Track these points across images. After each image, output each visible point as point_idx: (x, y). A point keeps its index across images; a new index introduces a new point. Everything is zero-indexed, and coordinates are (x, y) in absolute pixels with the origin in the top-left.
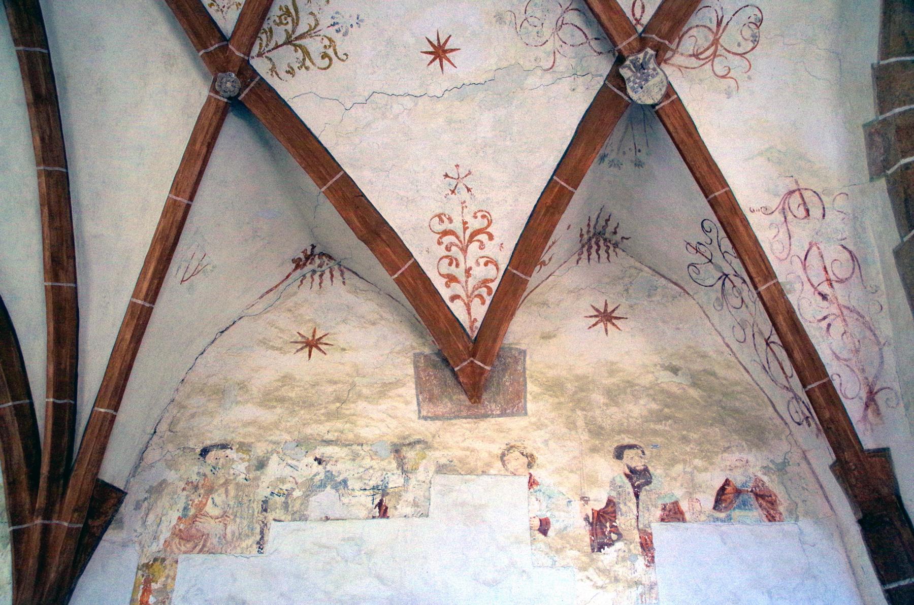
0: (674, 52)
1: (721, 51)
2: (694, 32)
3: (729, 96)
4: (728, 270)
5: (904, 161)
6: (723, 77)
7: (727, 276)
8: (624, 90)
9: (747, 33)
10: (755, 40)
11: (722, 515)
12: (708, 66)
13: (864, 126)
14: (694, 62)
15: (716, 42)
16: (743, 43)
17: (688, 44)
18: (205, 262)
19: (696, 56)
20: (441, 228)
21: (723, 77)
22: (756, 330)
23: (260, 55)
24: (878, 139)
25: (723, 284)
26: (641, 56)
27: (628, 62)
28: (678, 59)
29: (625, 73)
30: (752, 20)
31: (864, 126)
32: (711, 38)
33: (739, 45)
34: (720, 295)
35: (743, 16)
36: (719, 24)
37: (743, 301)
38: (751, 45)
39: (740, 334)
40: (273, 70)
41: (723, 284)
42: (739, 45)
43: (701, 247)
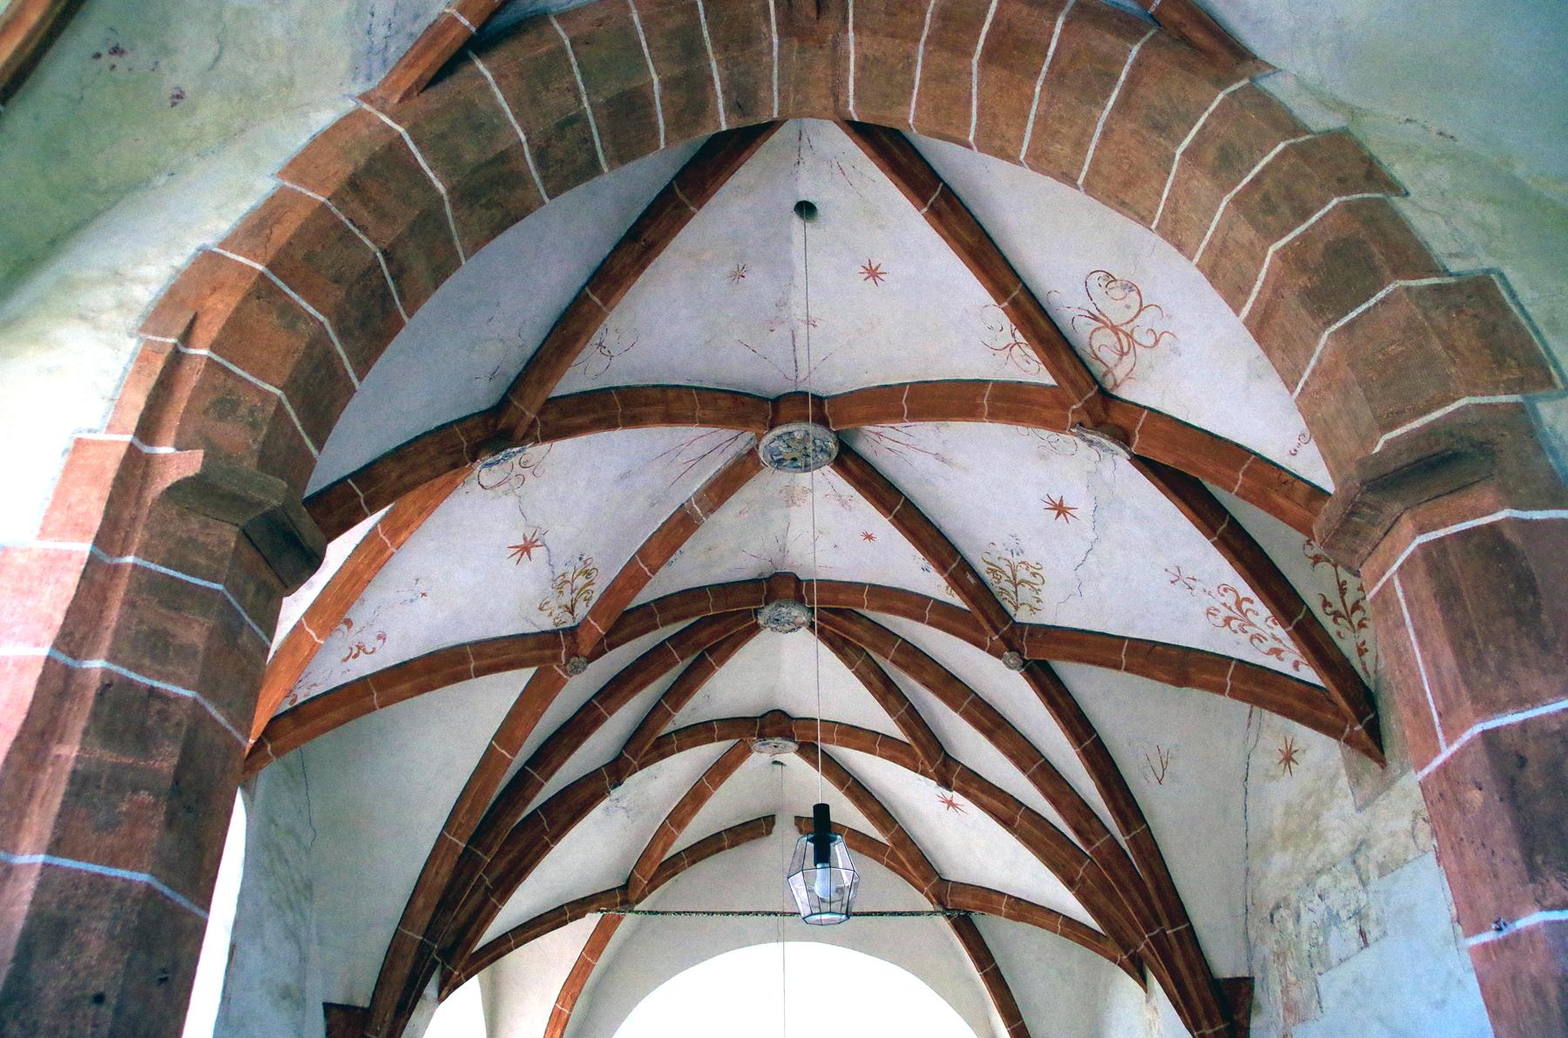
0: (1109, 371)
1: (1127, 329)
2: (1096, 345)
3: (1177, 352)
6: (1157, 342)
9: (1118, 293)
10: (1130, 287)
12: (1138, 349)
14: (1128, 361)
15: (1115, 329)
16: (1127, 301)
17: (1109, 357)
18: (1164, 750)
19: (1122, 354)
20: (1220, 621)
21: (1157, 342)
23: (1016, 608)
28: (1120, 373)
30: (1104, 284)
32: (1108, 331)
33: (1128, 307)
35: (1096, 291)
36: (1095, 318)
38: (1134, 294)
40: (1032, 609)
42: (1128, 307)
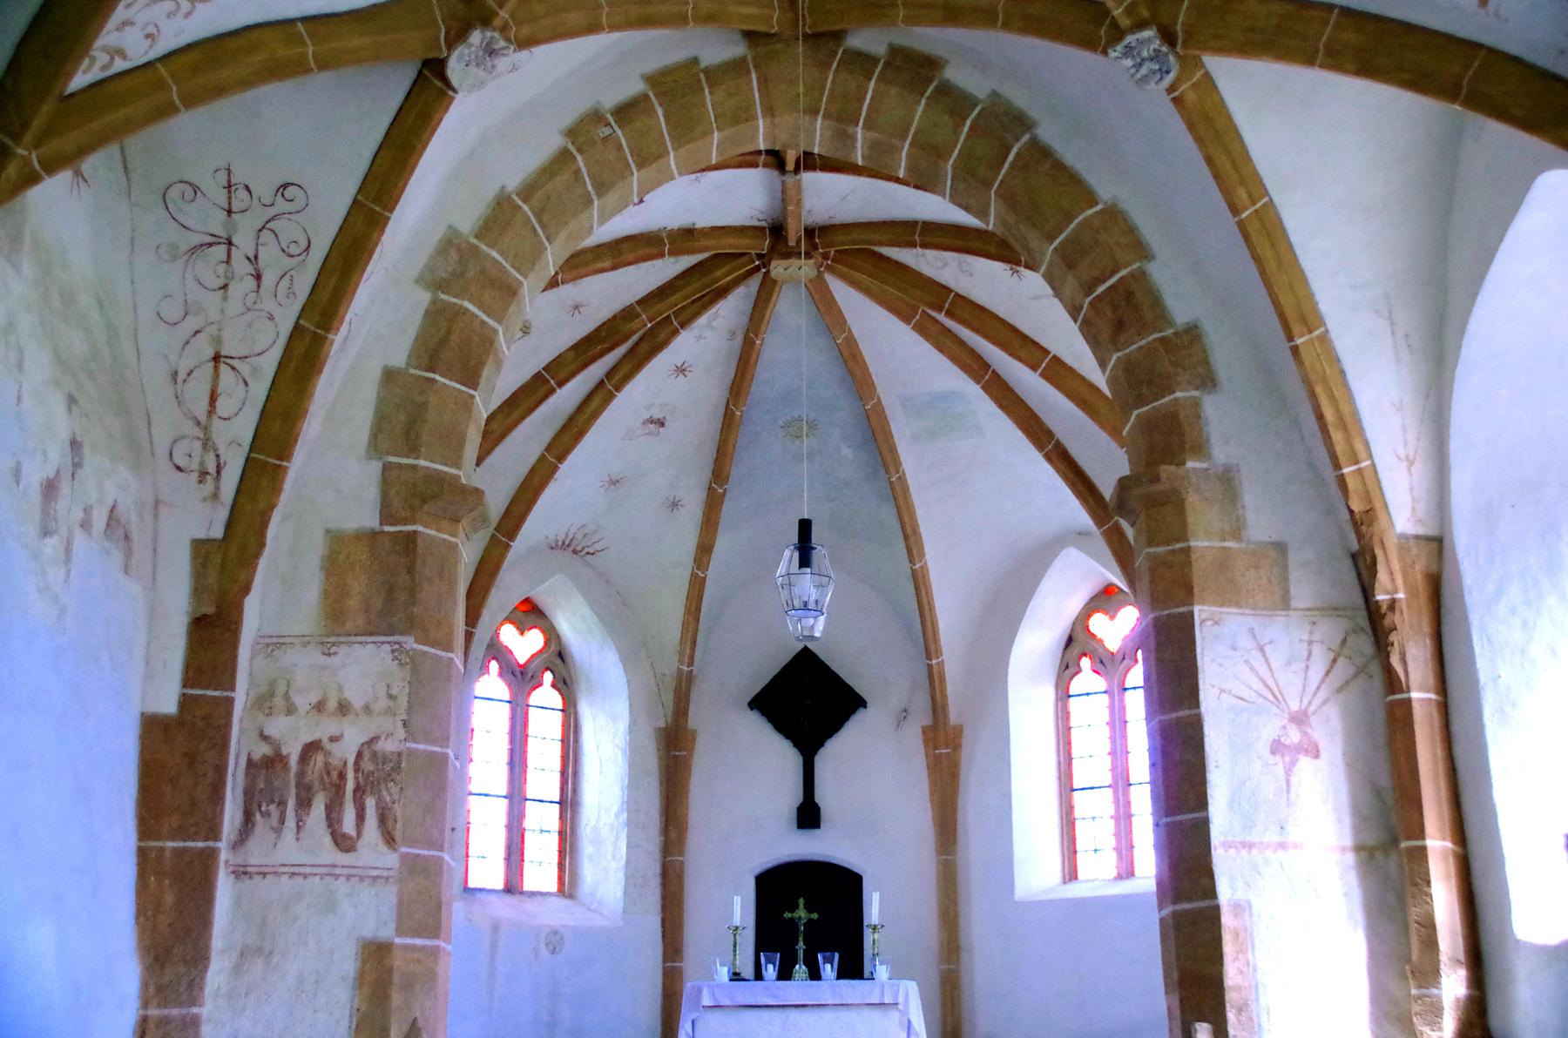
4: (244, 242)
5: (467, 304)
7: (230, 243)
8: (451, 46)
11: (107, 544)
13: (450, 227)
22: (213, 330)
24: (454, 256)
25: (211, 245)
26: (502, 43)
27: (489, 34)
29: (476, 37)
31: (450, 227)
34: (184, 247)
37: (225, 287)
39: (172, 311)
41: (211, 245)
43: (242, 193)
